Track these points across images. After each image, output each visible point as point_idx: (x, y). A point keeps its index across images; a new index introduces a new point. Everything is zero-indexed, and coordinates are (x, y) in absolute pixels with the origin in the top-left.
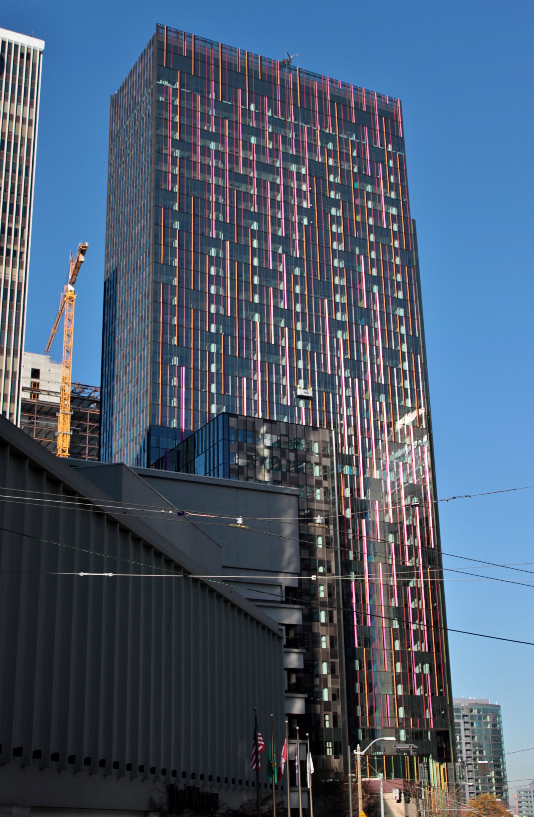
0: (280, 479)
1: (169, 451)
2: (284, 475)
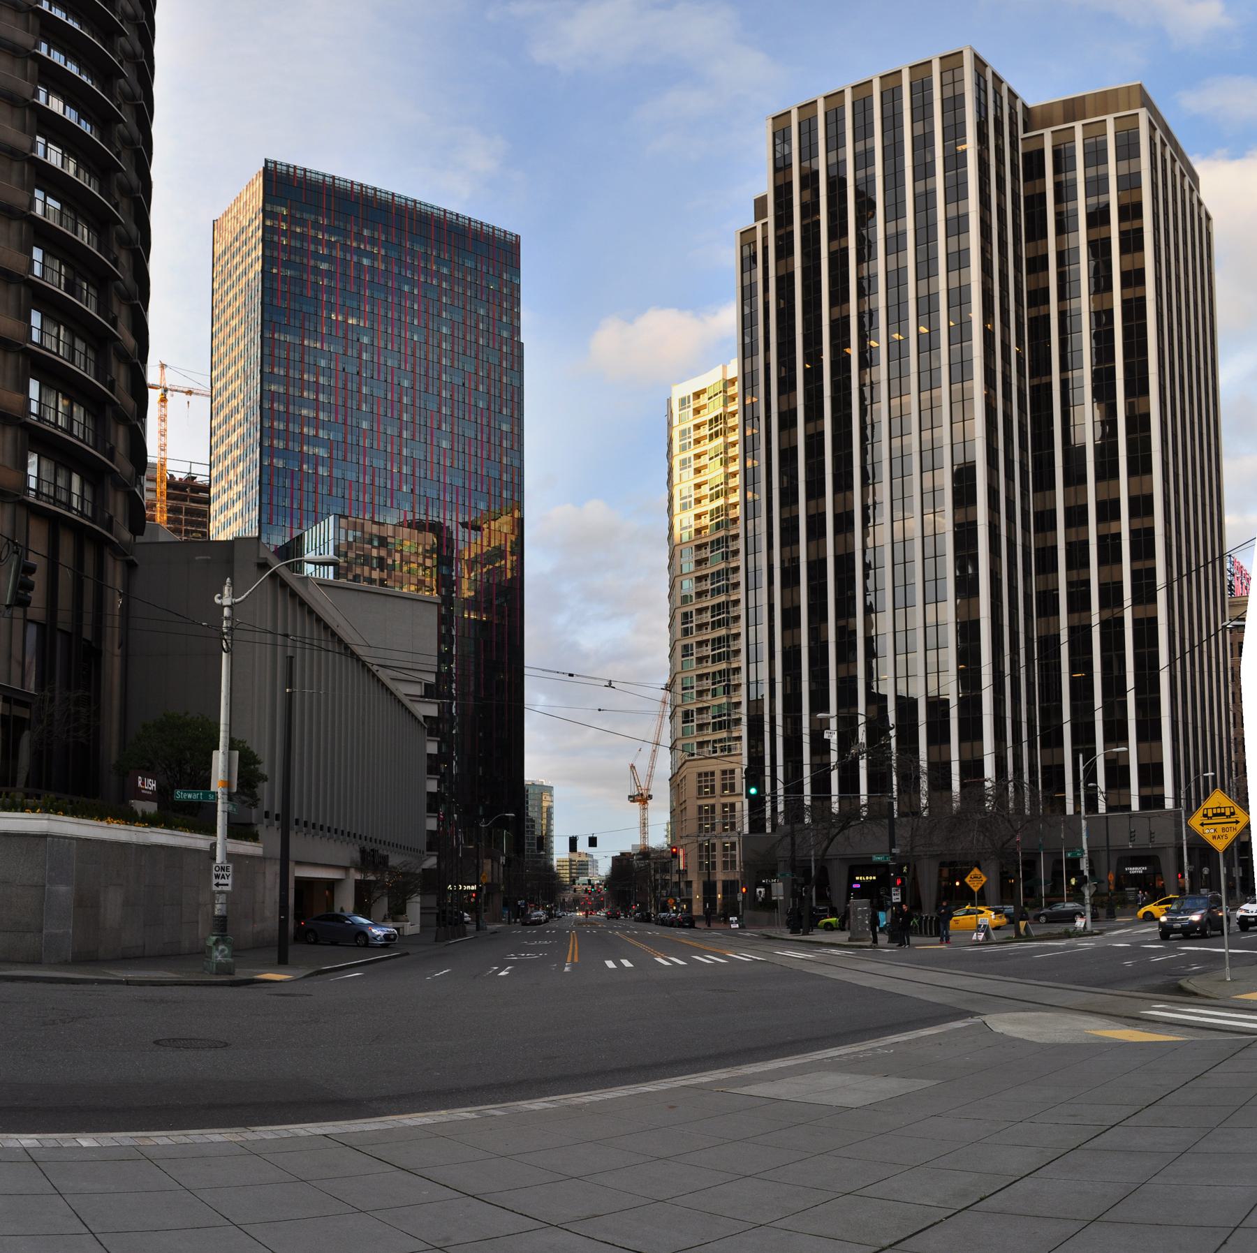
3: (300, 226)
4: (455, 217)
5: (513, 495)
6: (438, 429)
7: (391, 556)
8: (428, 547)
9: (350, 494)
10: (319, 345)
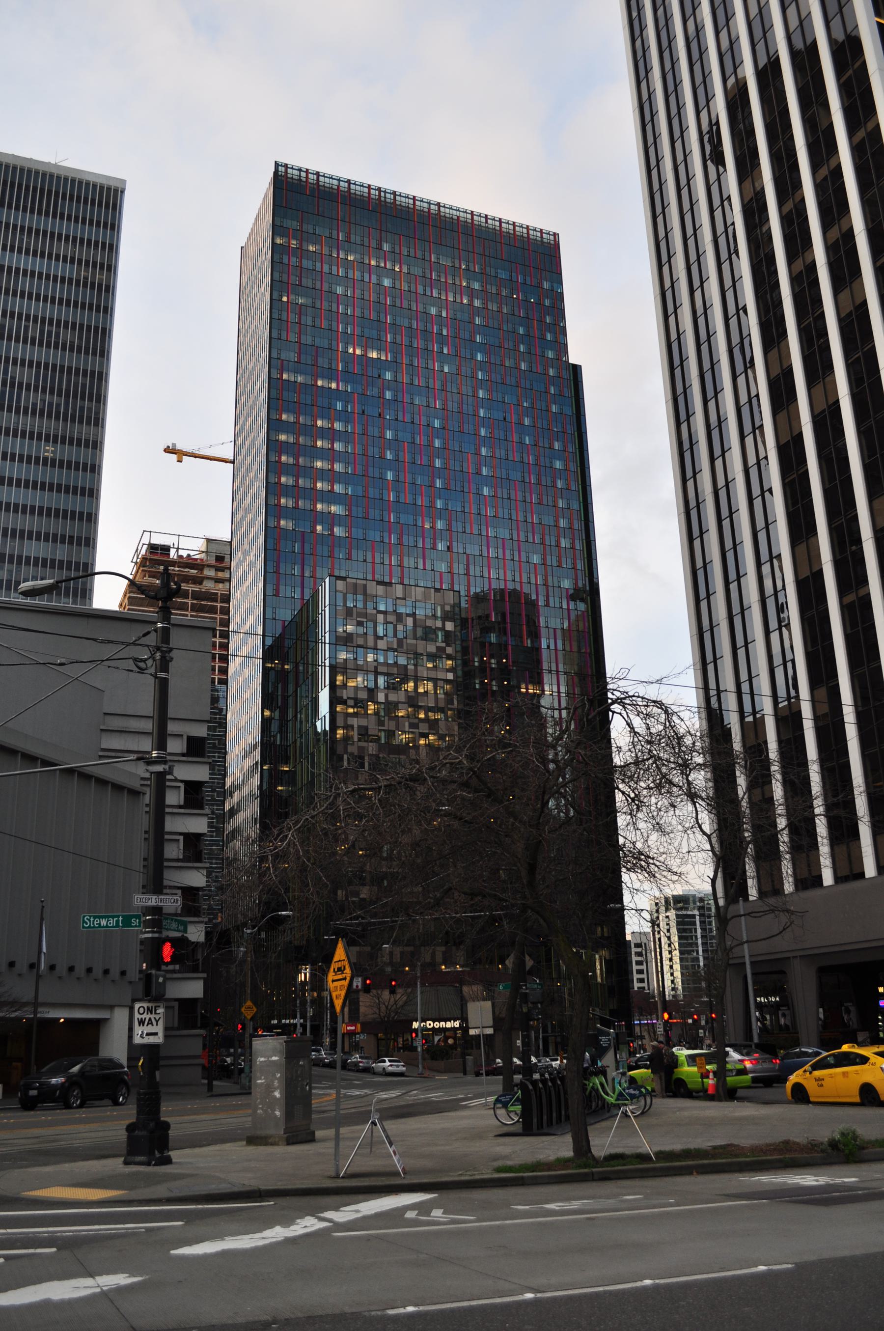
0: (395, 647)
1: (287, 623)
2: (400, 642)
3: (314, 244)
4: (483, 220)
5: (573, 543)
6: (477, 473)
7: (402, 621)
8: (447, 608)
9: (373, 558)
10: (334, 386)
